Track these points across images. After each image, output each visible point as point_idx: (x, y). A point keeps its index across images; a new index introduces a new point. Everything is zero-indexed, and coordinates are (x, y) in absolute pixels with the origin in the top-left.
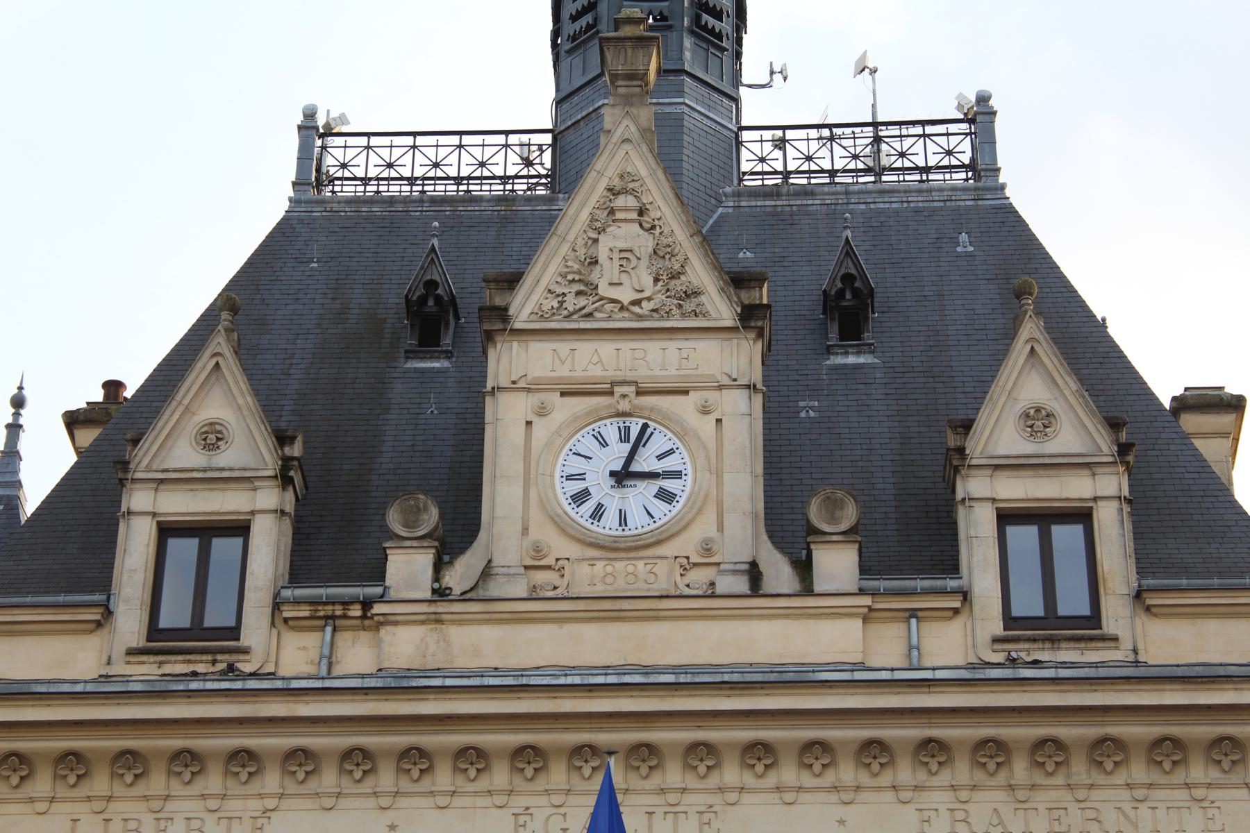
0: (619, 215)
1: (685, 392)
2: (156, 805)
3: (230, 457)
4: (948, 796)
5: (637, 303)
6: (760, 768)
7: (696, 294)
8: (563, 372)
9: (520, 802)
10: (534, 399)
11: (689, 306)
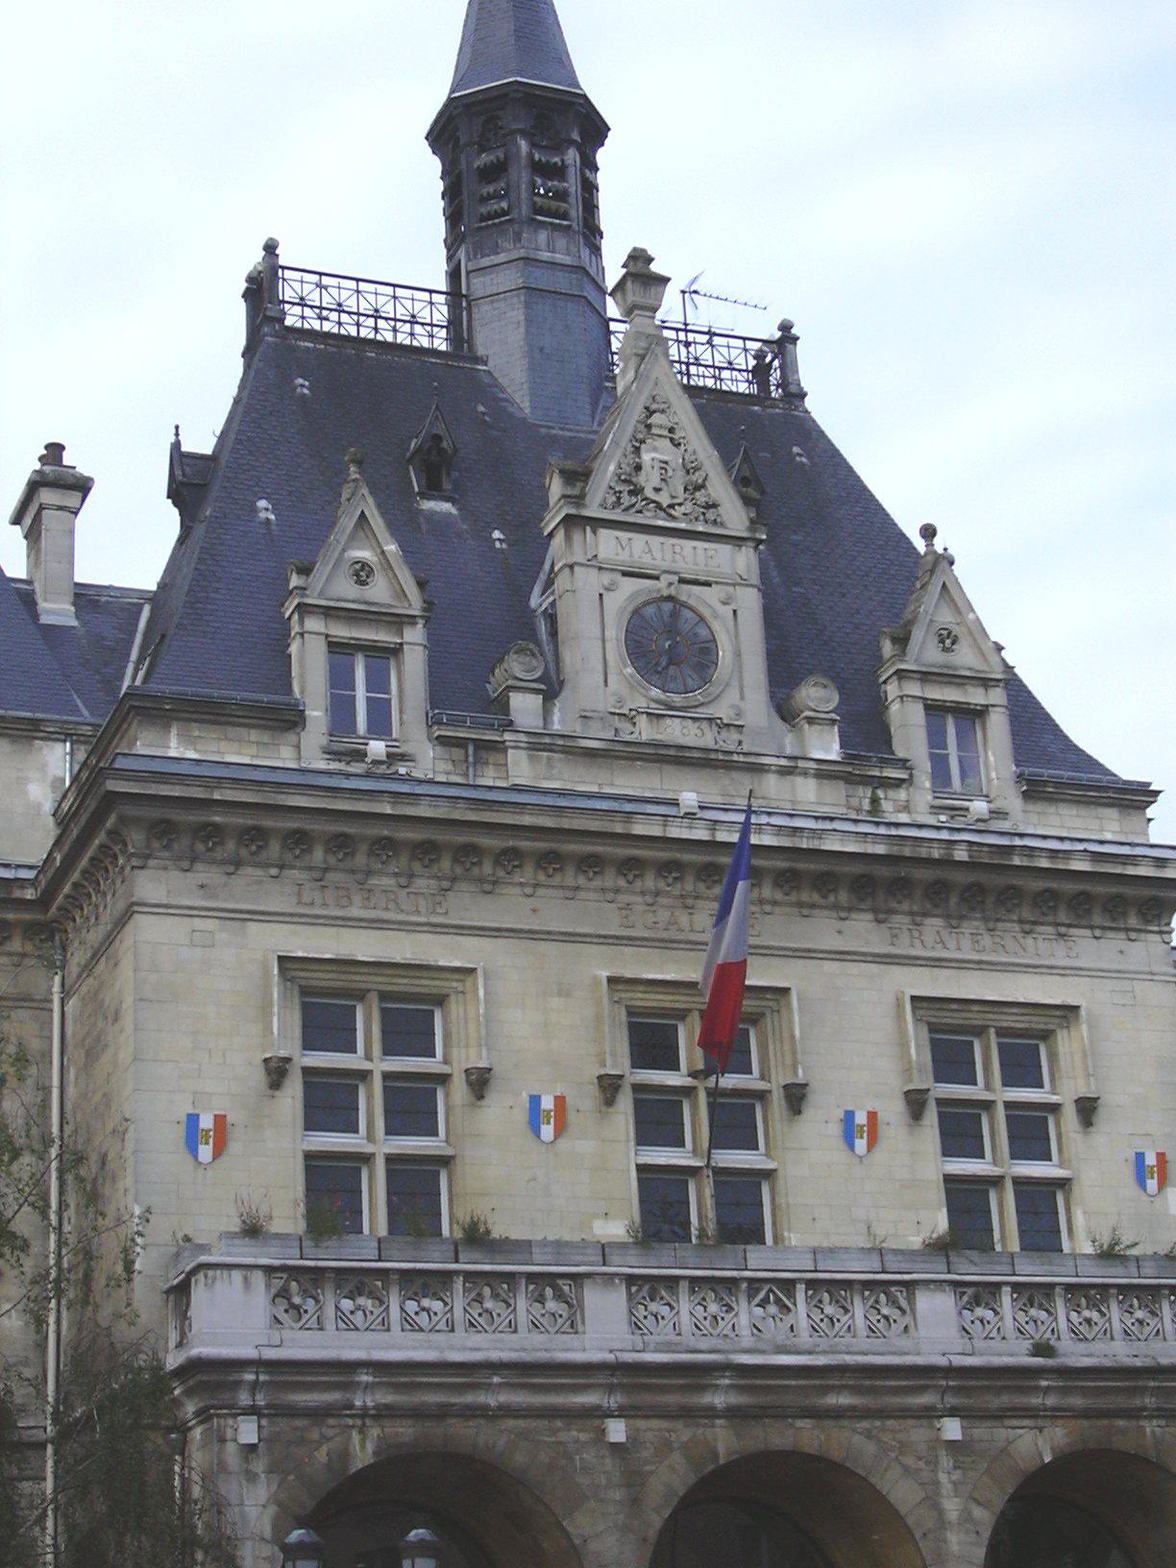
0: (654, 431)
1: (708, 584)
2: (359, 877)
3: (379, 592)
4: (907, 919)
5: (672, 506)
6: (786, 888)
7: (715, 506)
8: (624, 556)
9: (623, 898)
10: (606, 578)
11: (711, 515)
